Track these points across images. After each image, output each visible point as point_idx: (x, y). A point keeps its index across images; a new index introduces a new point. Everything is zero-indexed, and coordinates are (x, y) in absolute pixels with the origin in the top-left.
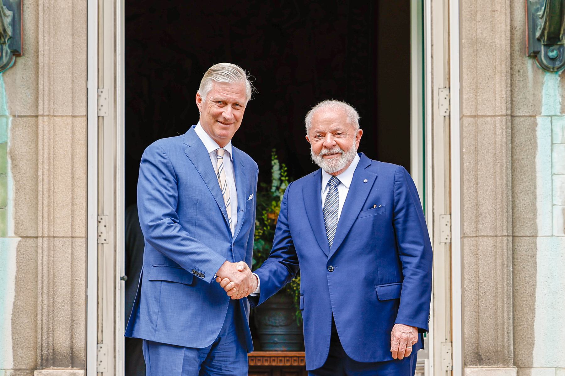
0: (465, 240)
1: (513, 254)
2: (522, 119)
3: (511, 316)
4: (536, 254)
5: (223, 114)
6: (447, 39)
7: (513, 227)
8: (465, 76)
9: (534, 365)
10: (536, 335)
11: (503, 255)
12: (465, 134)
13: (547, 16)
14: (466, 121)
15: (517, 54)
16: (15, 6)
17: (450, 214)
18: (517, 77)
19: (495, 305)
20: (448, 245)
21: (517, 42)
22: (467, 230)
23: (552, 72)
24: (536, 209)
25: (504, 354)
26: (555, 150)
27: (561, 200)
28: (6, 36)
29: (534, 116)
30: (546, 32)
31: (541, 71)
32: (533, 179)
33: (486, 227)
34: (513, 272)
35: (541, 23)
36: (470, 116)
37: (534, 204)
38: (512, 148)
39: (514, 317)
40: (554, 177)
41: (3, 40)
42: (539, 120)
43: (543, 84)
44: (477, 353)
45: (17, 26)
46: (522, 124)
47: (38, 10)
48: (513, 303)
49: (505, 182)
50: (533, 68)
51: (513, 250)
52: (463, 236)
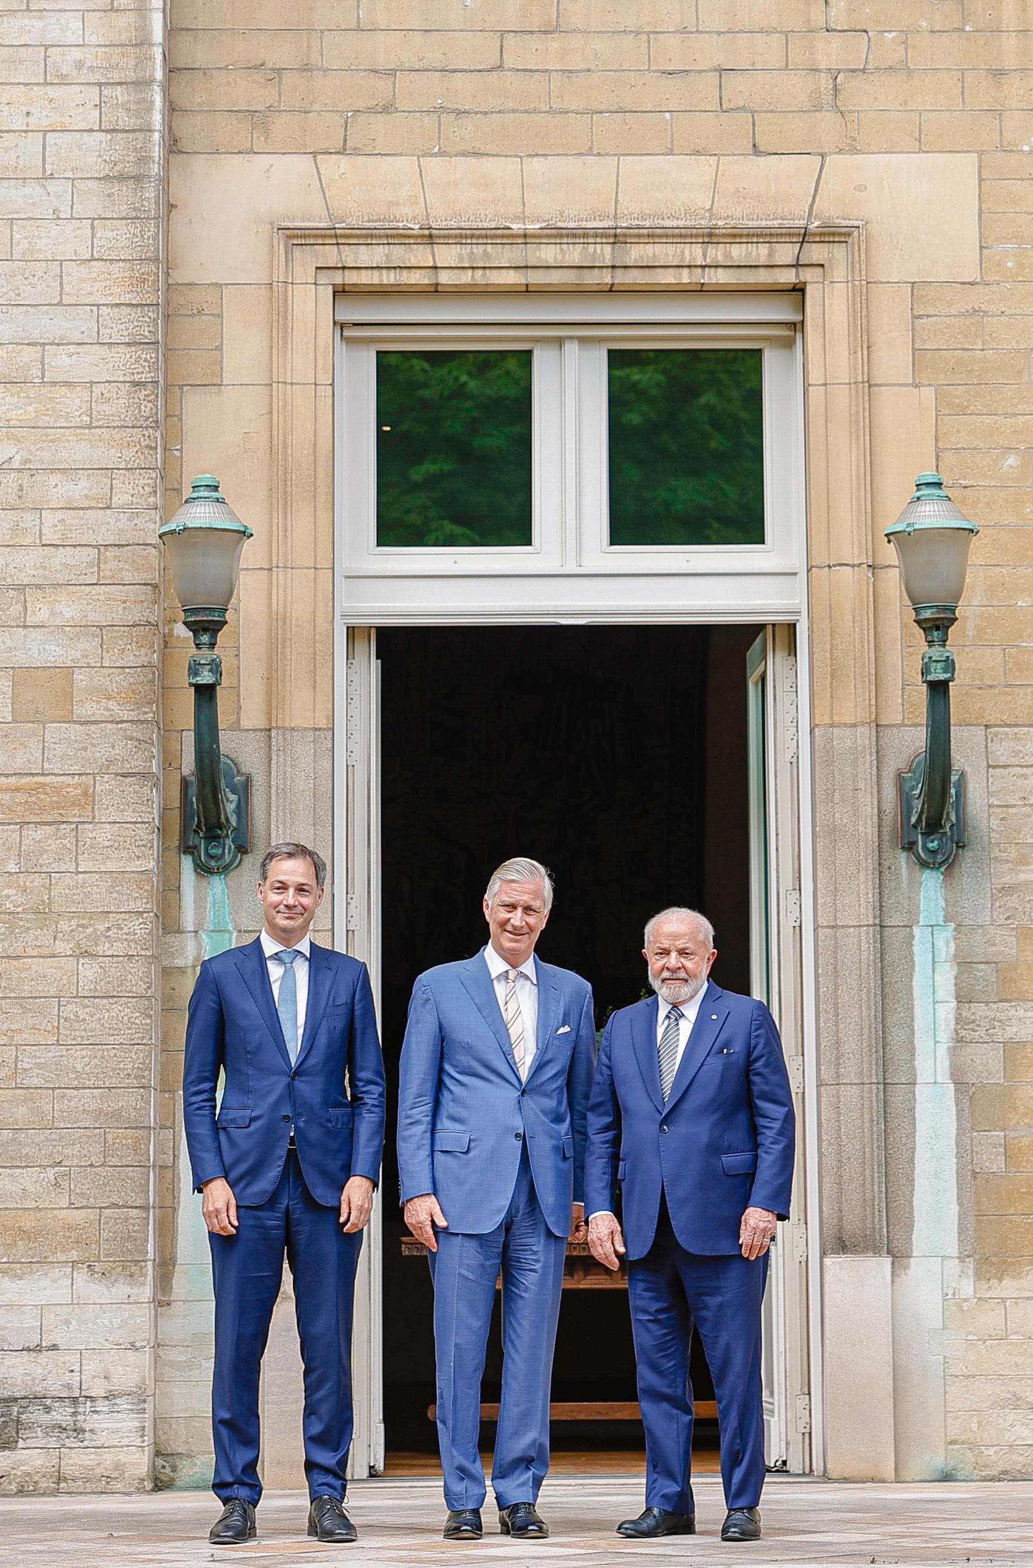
0: (823, 1089)
2: (895, 930)
3: (883, 1189)
4: (914, 1108)
5: (512, 921)
7: (884, 1072)
8: (819, 873)
9: (914, 1254)
10: (915, 1213)
11: (872, 1108)
12: (820, 951)
15: (886, 846)
16: (240, 788)
19: (863, 1174)
20: (800, 1094)
21: (886, 830)
23: (932, 868)
24: (914, 1048)
26: (937, 970)
29: (911, 927)
30: (924, 817)
32: (910, 1009)
33: (850, 1071)
34: (885, 1131)
35: (917, 805)
37: (912, 1042)
38: (882, 968)
40: (937, 1006)
42: (916, 931)
43: (921, 884)
44: (839, 1239)
45: (244, 814)
50: (907, 863)
51: (885, 1102)
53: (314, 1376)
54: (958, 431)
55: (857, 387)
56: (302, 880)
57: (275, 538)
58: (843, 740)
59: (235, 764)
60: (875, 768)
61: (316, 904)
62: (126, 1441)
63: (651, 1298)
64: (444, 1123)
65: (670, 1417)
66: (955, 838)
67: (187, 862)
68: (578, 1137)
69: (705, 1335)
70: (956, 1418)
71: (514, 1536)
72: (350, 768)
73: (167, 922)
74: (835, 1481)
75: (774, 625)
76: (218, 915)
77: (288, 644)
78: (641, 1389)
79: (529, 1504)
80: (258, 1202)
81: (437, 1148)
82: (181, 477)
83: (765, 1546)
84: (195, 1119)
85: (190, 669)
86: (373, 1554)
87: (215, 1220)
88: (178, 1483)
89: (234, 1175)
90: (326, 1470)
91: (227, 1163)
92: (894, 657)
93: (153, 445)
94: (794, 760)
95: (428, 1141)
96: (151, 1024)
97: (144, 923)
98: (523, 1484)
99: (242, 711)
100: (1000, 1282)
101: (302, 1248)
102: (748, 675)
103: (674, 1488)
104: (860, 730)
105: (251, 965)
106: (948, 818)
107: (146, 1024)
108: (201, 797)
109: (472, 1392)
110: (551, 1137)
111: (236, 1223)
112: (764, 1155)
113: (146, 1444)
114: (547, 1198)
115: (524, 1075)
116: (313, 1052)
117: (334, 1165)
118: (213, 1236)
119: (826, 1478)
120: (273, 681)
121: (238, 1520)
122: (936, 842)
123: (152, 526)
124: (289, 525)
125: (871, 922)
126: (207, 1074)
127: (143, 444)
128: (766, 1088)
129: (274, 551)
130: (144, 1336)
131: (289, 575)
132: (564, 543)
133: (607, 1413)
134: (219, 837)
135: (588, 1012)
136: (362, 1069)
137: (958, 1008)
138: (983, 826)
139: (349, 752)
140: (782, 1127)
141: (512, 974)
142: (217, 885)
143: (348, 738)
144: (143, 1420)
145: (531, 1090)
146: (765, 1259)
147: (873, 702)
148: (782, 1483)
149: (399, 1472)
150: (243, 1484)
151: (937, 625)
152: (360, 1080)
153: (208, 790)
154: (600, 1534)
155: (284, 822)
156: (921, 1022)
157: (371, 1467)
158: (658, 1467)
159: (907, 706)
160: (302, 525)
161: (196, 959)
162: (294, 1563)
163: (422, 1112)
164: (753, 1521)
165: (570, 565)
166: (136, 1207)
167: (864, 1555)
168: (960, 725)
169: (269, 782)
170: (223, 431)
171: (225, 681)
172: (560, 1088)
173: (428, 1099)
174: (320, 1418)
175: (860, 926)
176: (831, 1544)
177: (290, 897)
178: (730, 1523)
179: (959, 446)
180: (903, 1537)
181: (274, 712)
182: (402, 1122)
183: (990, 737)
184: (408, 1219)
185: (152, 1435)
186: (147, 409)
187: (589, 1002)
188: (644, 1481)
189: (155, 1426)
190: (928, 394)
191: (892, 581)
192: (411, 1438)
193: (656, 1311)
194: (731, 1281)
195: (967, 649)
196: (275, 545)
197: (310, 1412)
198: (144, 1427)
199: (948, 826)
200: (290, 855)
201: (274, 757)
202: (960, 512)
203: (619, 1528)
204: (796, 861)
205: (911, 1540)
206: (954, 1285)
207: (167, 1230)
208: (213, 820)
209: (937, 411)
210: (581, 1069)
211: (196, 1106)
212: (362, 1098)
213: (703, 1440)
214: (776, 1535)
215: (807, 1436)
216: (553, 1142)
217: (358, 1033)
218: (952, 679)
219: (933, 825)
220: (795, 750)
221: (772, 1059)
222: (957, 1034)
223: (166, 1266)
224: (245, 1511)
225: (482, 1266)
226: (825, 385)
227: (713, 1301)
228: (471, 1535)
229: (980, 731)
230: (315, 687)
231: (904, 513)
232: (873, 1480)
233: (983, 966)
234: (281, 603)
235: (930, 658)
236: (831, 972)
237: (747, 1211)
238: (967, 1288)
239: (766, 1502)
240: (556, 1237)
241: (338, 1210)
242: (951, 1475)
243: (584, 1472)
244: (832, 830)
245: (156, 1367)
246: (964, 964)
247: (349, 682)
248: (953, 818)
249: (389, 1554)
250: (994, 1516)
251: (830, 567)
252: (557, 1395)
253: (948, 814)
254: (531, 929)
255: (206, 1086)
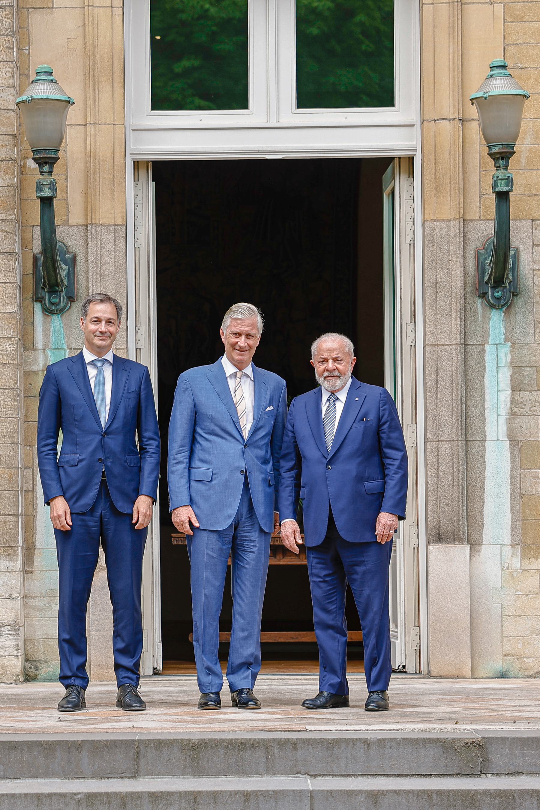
0: (428, 444)
1: (466, 454)
3: (465, 504)
4: (485, 455)
6: (413, 284)
7: (466, 434)
8: (427, 312)
11: (458, 455)
13: (493, 263)
14: (428, 349)
15: (469, 295)
17: (416, 424)
18: (469, 313)
19: (453, 495)
21: (468, 285)
22: (429, 436)
24: (484, 419)
25: (460, 534)
26: (500, 371)
27: (504, 412)
28: (63, 285)
30: (492, 277)
31: (488, 308)
32: (483, 396)
33: (445, 434)
35: (488, 269)
36: (431, 345)
37: (483, 415)
38: (466, 370)
39: (467, 505)
41: (61, 288)
42: (487, 347)
43: (490, 319)
46: (473, 351)
47: (88, 264)
48: (467, 494)
49: (460, 397)
50: (482, 306)
52: (426, 441)
53: (121, 612)
54: (518, 33)
55: (453, 5)
56: (110, 316)
57: (88, 103)
58: (443, 229)
59: (66, 247)
60: (462, 247)
61: (117, 331)
62: (7, 653)
63: (321, 568)
64: (196, 463)
65: (334, 638)
66: (512, 290)
67: (38, 307)
68: (277, 473)
69: (353, 589)
70: (509, 641)
71: (240, 708)
72: (137, 249)
73: (26, 343)
74: (435, 677)
75: (400, 158)
76: (56, 339)
77: (97, 172)
78: (316, 622)
79: (249, 689)
80: (84, 510)
81: (193, 478)
82: (29, 67)
83: (391, 714)
84: (45, 461)
85: (37, 187)
86: (155, 718)
87: (58, 522)
88: (39, 677)
89: (68, 495)
90: (127, 669)
91: (64, 487)
92: (475, 178)
93: (11, 46)
94: (412, 242)
95: (186, 474)
96: (17, 405)
97: (12, 344)
98: (245, 678)
99: (71, 213)
100: (537, 560)
101: (109, 539)
102: (384, 189)
103: (336, 680)
104: (453, 223)
105: (77, 368)
106: (508, 278)
107: (15, 405)
108: (46, 267)
109: (215, 624)
110: (262, 473)
111: (70, 523)
112: (389, 481)
113: (19, 654)
114: (260, 509)
115: (246, 435)
116: (116, 421)
117: (129, 488)
118: (56, 531)
119: (429, 675)
120: (88, 195)
121: (75, 698)
122: (500, 293)
123: (12, 98)
124: (97, 97)
125: (459, 342)
126: (51, 434)
127: (5, 46)
128: (390, 441)
129: (88, 114)
130: (17, 591)
131: (97, 129)
132: (268, 107)
133: (297, 638)
134: (57, 291)
135: (284, 398)
136: (146, 430)
137: (512, 395)
138: (530, 283)
139: (136, 239)
140: (400, 464)
141: (239, 374)
142: (56, 321)
143: (135, 230)
144: (17, 640)
145: (250, 444)
146: (390, 544)
147: (461, 206)
148: (402, 678)
149: (170, 672)
150: (77, 677)
151: (502, 156)
152: (145, 437)
153: (49, 263)
154: (291, 707)
155: (97, 282)
156: (489, 403)
157: (154, 669)
158: (327, 668)
159: (483, 208)
160: (104, 98)
161: (44, 366)
162: (108, 722)
163: (183, 456)
164: (384, 699)
165: (273, 122)
166: (11, 515)
167: (452, 719)
168: (516, 220)
169: (87, 258)
170: (54, 36)
171: (59, 195)
172: (267, 443)
173: (187, 448)
174: (123, 641)
175: (452, 345)
176: (431, 713)
177: (103, 327)
178: (370, 700)
179: (518, 42)
180: (475, 709)
181: (89, 214)
182: (171, 461)
183: (534, 227)
184: (174, 519)
185: (23, 649)
186: (7, 23)
187: (284, 392)
188: (318, 677)
189: (25, 644)
190: (499, 9)
191: (474, 128)
192: (178, 652)
193: (326, 576)
194: (370, 558)
195: (521, 172)
196: (88, 110)
197: (116, 635)
198: (18, 645)
199: (507, 282)
200: (102, 301)
201: (90, 242)
202: (518, 84)
203: (304, 703)
204: (413, 305)
205: (480, 711)
206: (508, 561)
207: (30, 529)
208: (53, 281)
209: (504, 19)
210: (279, 431)
211: (45, 453)
212: (146, 448)
213: (354, 654)
214: (398, 708)
215: (418, 651)
216: (263, 476)
217: (143, 409)
218: (511, 190)
219: (498, 282)
220: (412, 236)
221: (393, 423)
222: (511, 409)
223: (30, 551)
224: (79, 692)
225: (221, 549)
226: (433, 4)
227: (360, 569)
228: (214, 707)
229: (529, 223)
230: (114, 199)
231: (482, 86)
232: (458, 677)
233: (528, 369)
234: (93, 147)
235: (498, 177)
236: (433, 373)
237: (380, 515)
238: (516, 563)
239: (392, 689)
240: (266, 533)
241: (131, 516)
242: (505, 674)
243: (282, 672)
244: (435, 285)
245: (25, 610)
246: (516, 367)
247: (136, 196)
248: (511, 278)
249: (165, 718)
250: (531, 697)
251: (435, 120)
252: (266, 626)
253: (508, 275)
254: (251, 347)
255: (51, 441)
